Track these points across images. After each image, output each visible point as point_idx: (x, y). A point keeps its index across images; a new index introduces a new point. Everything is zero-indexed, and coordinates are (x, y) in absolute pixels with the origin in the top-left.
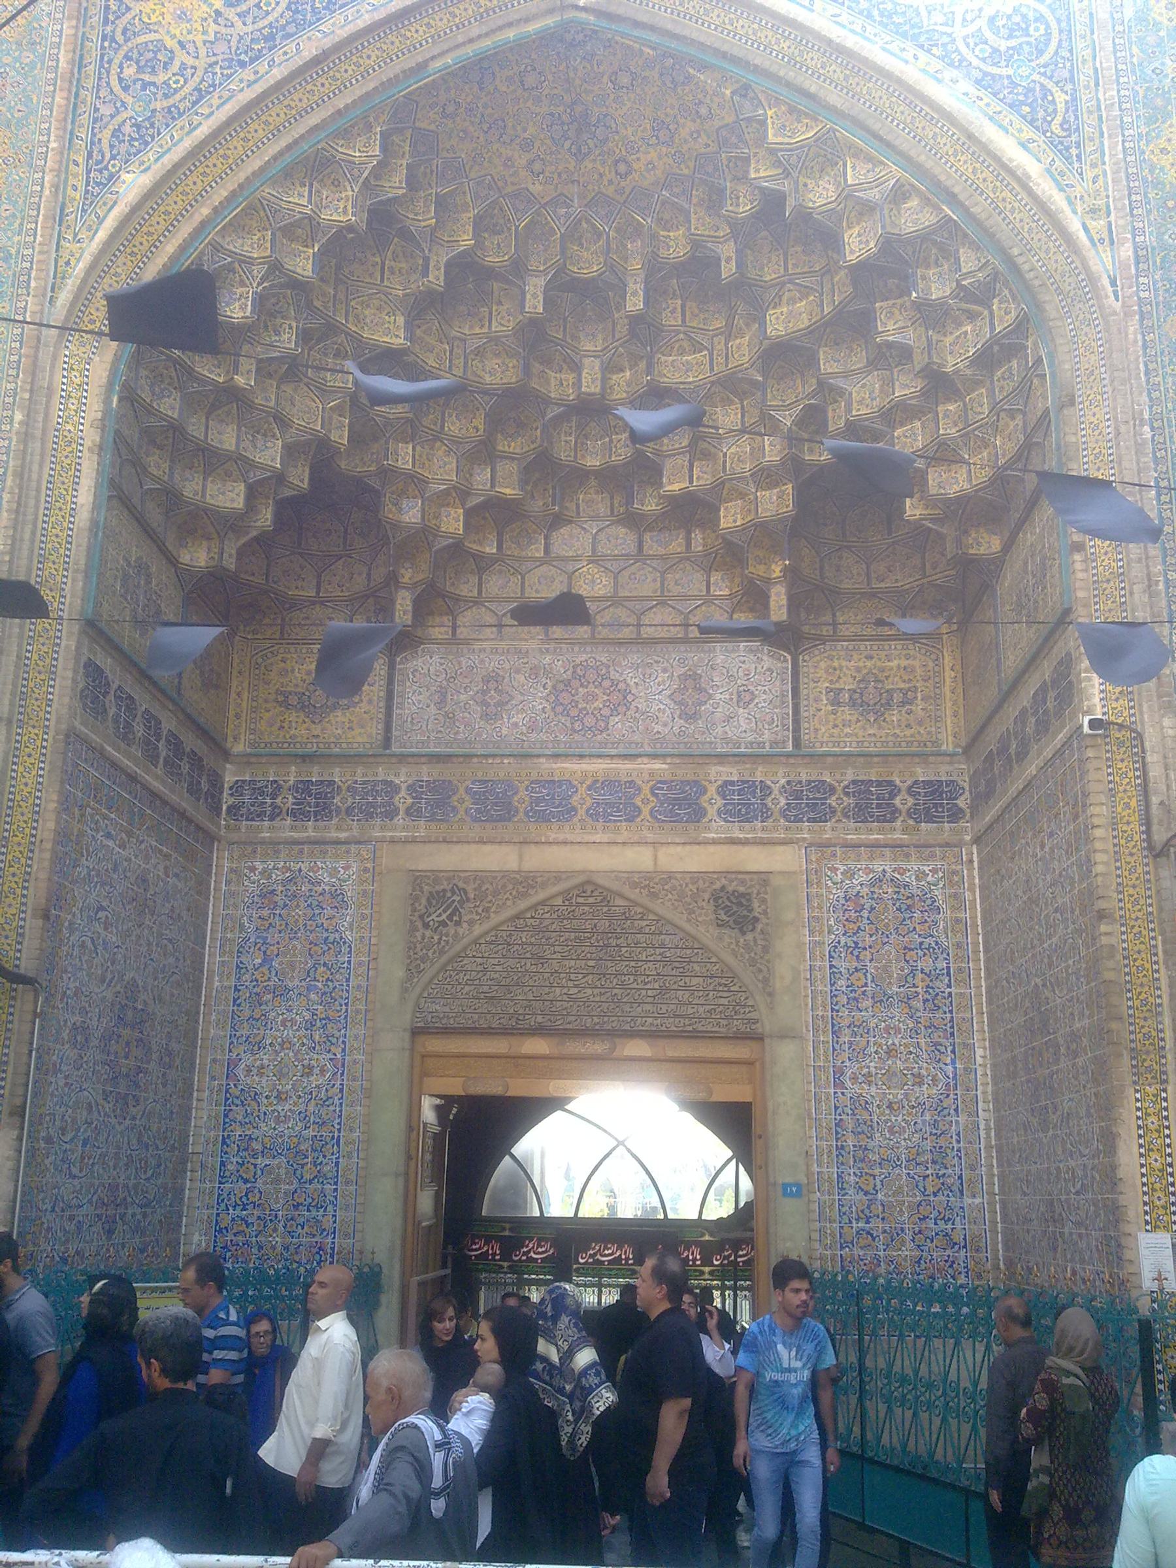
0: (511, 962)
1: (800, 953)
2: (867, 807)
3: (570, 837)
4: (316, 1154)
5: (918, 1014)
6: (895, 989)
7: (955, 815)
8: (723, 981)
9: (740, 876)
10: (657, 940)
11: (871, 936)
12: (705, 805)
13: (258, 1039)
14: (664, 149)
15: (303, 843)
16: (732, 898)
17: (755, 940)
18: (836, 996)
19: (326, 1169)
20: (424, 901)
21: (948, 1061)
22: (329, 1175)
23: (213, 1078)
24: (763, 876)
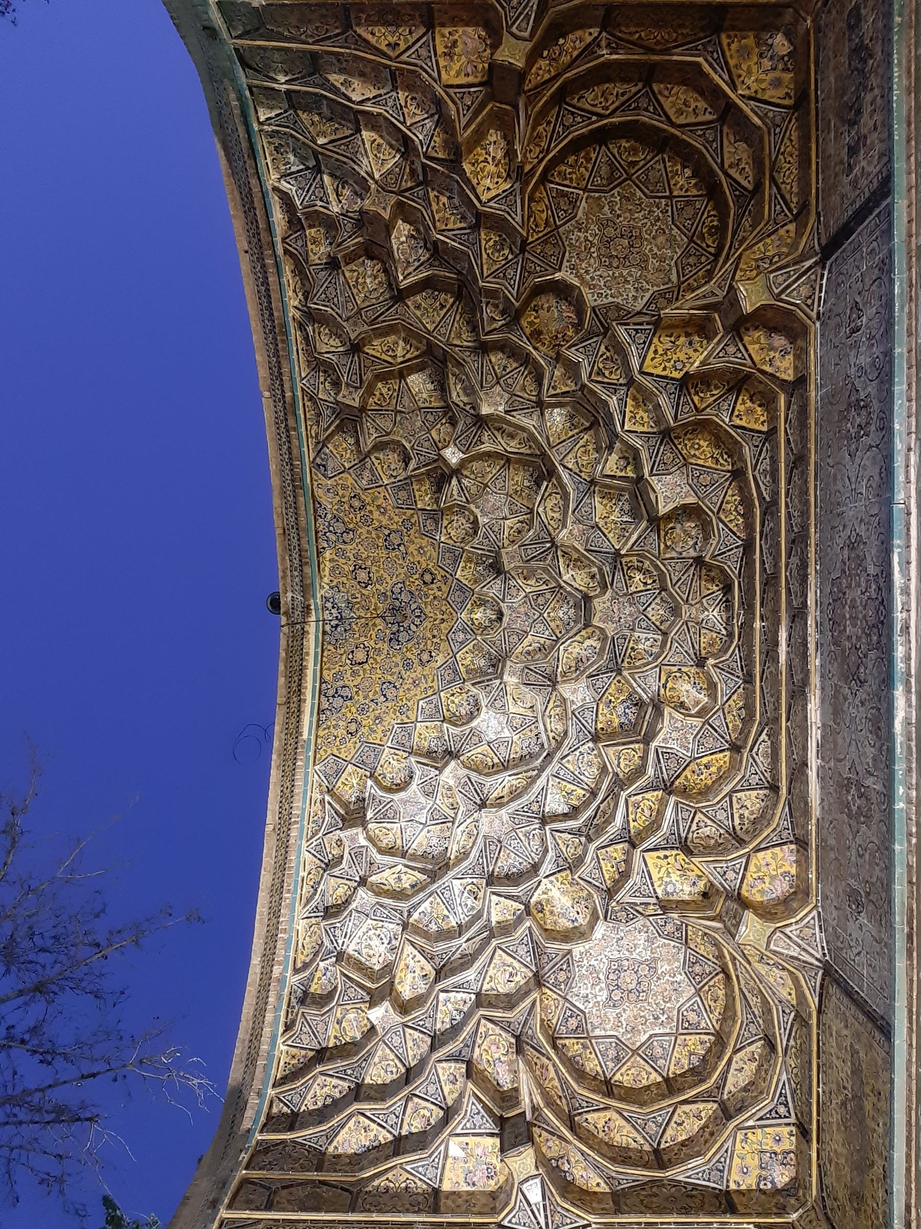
14: (406, 538)
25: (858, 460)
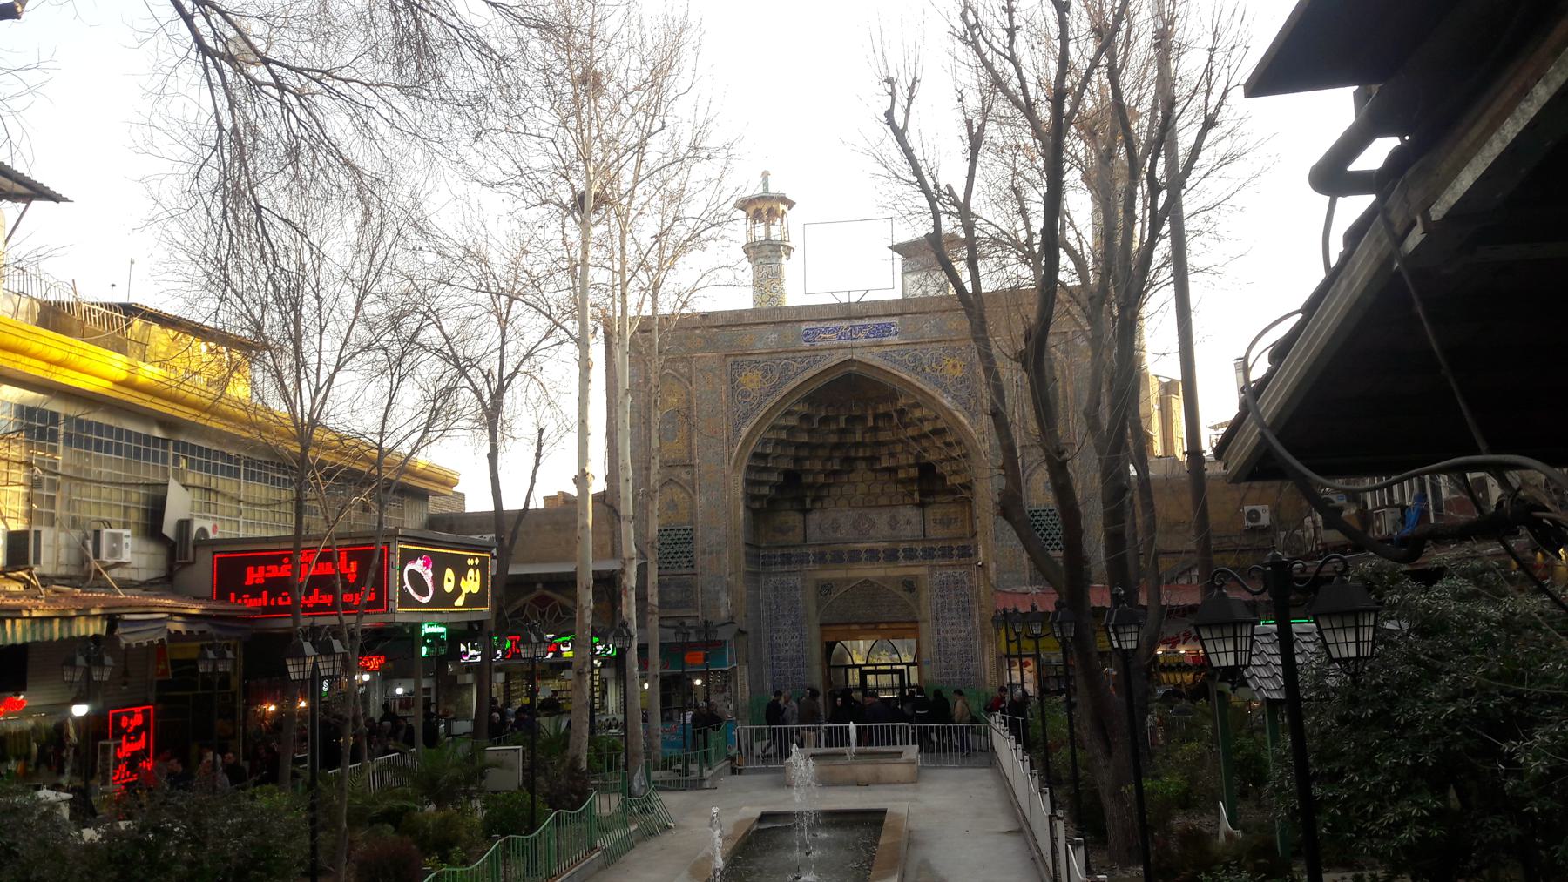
1: (927, 596)
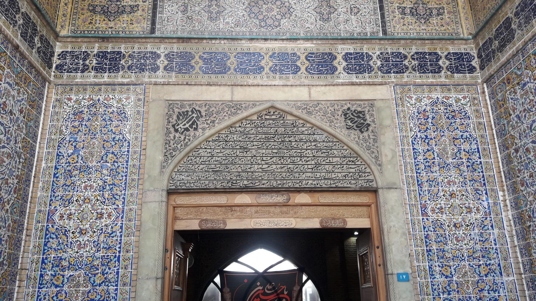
0: (227, 151)
2: (425, 65)
3: (261, 82)
4: (104, 267)
5: (465, 174)
6: (450, 160)
7: (472, 70)
8: (352, 159)
9: (357, 103)
10: (312, 138)
11: (434, 132)
12: (336, 65)
13: (68, 197)
15: (101, 85)
16: (354, 114)
17: (369, 136)
18: (418, 165)
19: (110, 276)
20: (175, 117)
21: (484, 199)
22: (113, 280)
23: (39, 222)
24: (370, 102)
25: (313, 12)
